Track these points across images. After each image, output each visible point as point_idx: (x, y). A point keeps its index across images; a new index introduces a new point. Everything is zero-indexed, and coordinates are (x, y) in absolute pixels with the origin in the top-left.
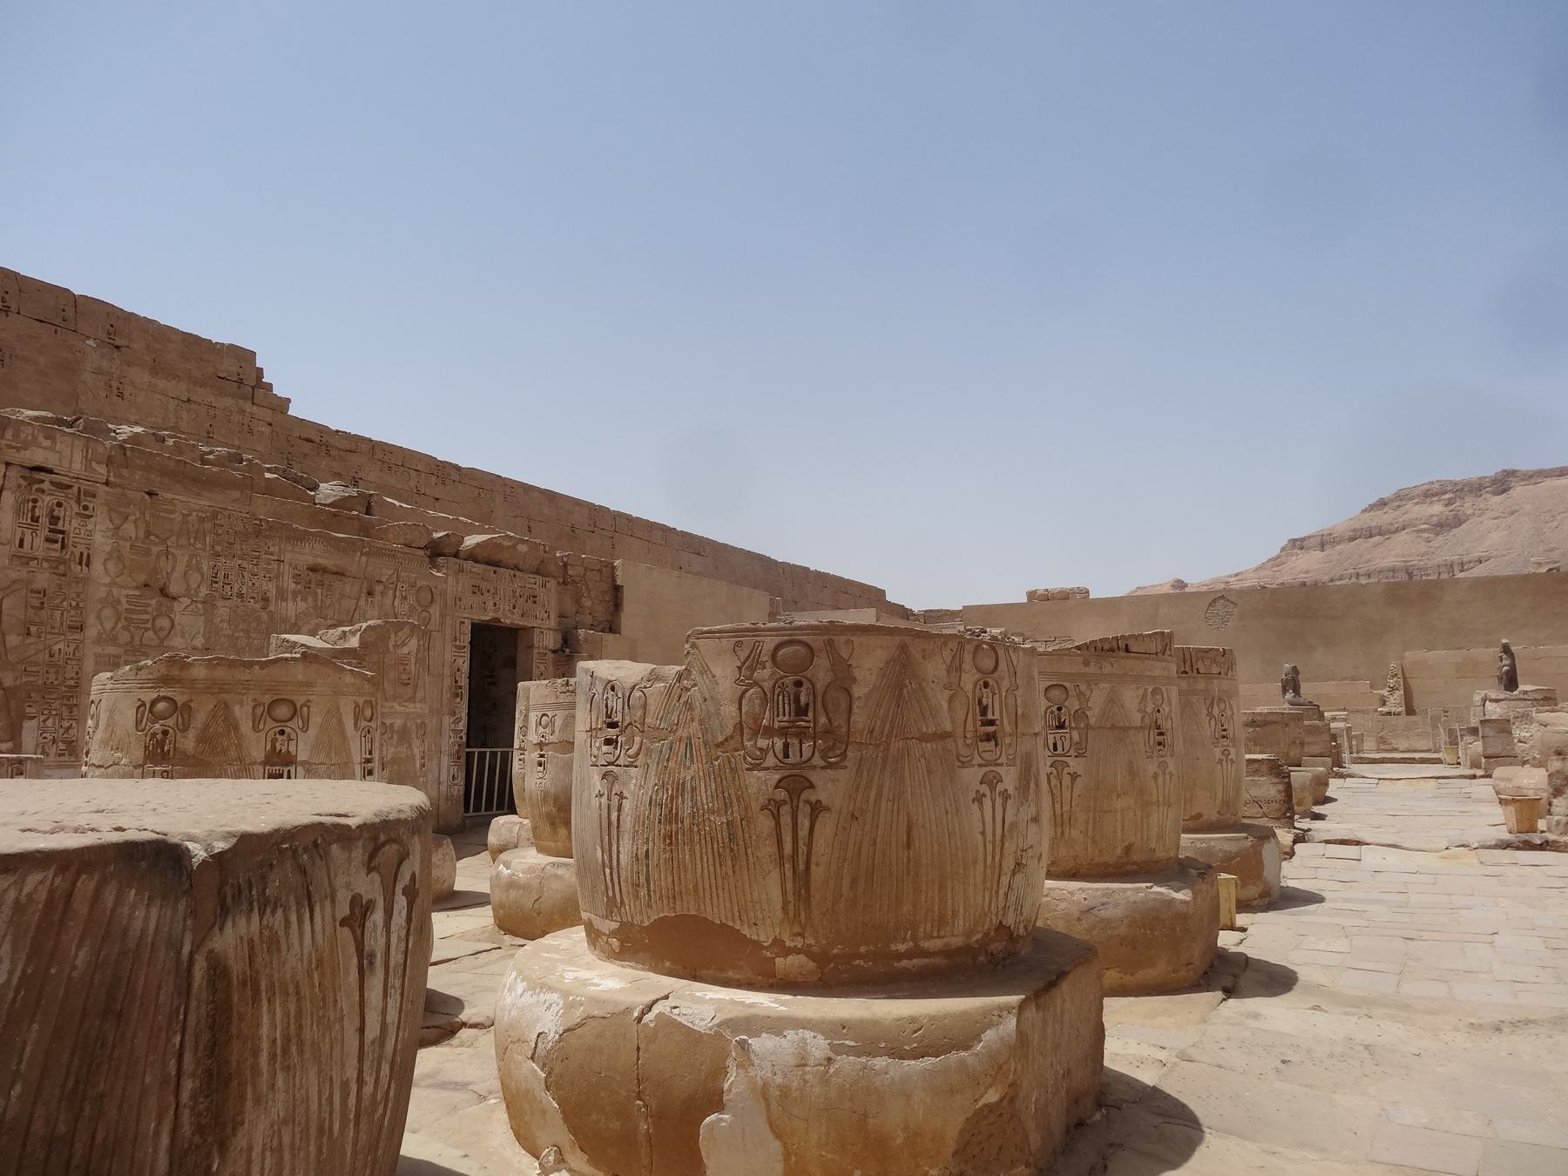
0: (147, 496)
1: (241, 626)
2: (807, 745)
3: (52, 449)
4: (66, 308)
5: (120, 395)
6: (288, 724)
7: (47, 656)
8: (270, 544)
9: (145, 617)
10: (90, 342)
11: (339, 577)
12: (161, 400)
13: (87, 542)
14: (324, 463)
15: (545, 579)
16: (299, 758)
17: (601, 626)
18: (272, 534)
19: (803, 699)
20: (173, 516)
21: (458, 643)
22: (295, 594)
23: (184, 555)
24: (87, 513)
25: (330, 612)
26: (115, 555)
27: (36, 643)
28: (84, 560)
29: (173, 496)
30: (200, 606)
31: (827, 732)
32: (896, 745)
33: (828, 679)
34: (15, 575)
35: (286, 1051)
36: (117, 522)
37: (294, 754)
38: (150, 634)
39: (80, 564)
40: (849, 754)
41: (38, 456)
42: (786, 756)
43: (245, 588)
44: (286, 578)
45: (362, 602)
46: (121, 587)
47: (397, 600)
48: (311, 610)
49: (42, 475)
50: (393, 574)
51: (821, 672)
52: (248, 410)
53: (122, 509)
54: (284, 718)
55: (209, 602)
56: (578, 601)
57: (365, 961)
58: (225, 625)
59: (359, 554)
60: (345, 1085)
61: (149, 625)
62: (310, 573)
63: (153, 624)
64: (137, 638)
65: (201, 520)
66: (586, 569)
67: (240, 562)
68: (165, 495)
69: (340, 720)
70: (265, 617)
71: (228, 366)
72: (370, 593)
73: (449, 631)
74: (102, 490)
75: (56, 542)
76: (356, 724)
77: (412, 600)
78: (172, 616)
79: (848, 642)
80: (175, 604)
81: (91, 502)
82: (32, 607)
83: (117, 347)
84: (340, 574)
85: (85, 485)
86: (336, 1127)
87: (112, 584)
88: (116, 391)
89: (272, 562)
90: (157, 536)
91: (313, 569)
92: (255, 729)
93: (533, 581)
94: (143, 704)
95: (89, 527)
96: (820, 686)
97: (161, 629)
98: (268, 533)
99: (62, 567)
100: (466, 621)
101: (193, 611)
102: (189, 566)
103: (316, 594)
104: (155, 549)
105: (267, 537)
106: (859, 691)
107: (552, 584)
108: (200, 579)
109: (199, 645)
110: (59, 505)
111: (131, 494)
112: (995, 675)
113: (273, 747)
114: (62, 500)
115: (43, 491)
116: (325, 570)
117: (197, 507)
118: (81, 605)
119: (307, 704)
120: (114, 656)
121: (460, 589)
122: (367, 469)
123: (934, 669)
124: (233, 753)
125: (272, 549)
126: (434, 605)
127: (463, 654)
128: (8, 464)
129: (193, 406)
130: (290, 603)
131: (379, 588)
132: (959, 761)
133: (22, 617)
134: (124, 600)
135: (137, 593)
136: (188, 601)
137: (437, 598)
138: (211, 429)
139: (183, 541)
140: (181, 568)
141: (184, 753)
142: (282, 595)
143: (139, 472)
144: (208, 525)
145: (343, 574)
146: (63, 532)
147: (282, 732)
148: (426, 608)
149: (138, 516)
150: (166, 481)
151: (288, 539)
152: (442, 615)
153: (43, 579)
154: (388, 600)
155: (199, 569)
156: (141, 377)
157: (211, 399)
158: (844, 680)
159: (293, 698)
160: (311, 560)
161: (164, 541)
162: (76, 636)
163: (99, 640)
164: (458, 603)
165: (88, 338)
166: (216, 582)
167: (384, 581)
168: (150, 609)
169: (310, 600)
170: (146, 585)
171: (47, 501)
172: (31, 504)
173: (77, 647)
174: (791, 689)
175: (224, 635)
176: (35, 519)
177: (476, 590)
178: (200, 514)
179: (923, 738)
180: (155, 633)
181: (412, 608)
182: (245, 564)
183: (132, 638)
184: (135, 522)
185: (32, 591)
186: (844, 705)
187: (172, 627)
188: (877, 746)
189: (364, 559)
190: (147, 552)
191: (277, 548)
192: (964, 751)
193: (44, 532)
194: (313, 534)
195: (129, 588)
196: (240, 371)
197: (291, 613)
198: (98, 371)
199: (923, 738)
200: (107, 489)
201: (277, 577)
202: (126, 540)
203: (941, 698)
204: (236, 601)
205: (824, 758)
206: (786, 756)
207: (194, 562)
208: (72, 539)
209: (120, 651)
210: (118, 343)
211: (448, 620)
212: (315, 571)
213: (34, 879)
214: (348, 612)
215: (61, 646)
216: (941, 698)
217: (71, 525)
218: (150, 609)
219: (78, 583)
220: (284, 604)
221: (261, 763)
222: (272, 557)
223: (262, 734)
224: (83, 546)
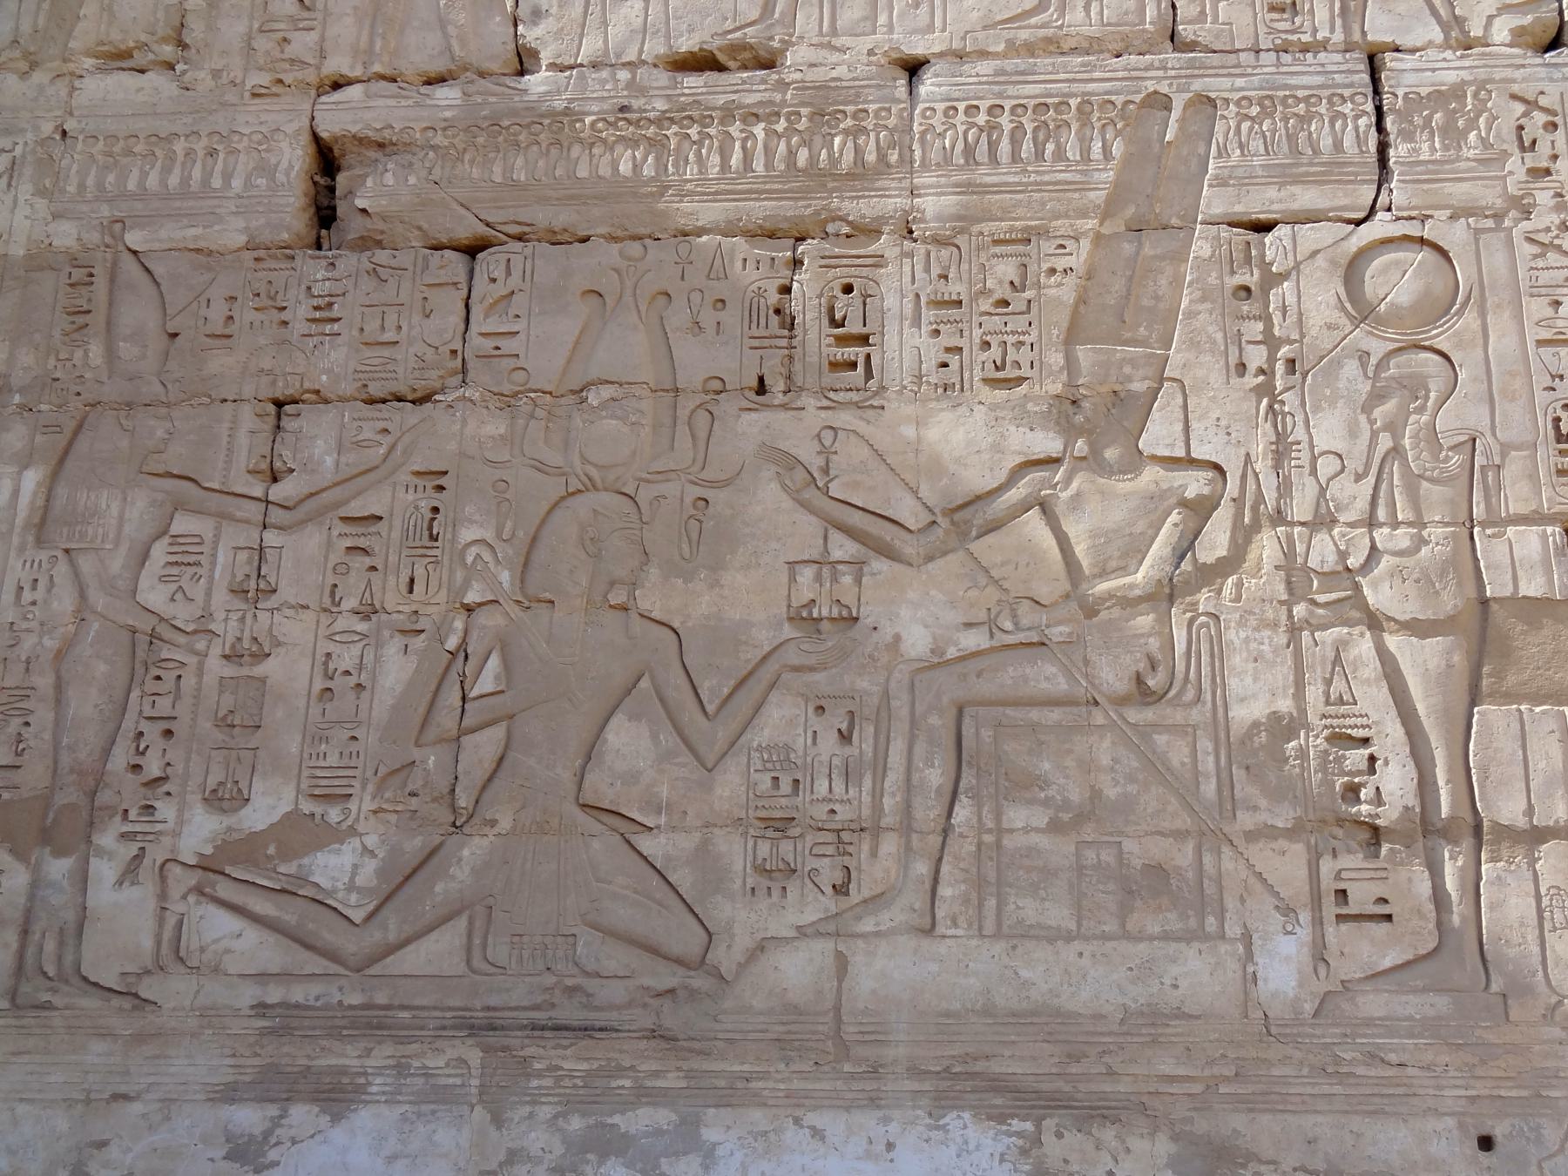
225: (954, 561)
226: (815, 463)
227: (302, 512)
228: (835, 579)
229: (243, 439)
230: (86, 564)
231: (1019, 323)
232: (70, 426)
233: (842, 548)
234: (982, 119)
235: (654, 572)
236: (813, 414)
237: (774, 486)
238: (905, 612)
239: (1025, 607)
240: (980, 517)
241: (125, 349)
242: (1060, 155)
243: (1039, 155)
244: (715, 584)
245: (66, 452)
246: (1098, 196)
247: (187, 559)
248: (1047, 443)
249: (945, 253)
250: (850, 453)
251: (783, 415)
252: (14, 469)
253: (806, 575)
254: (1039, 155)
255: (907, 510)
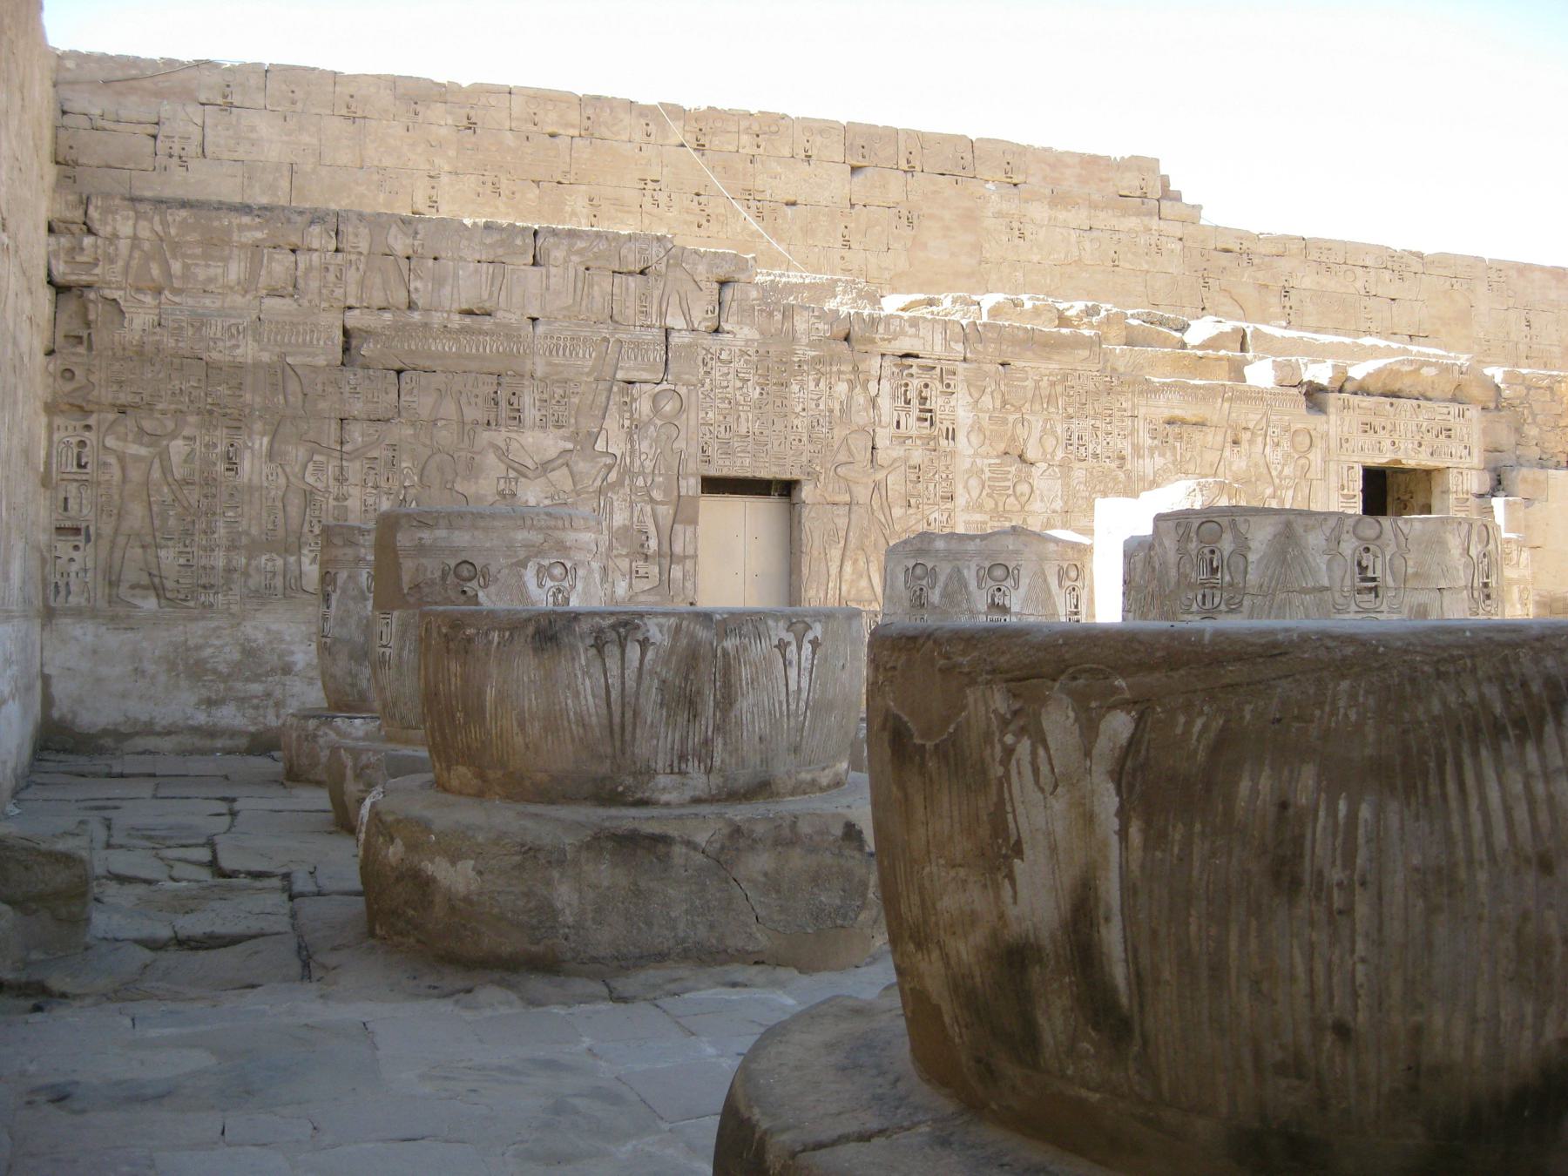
0: (1000, 367)
1: (1098, 488)
2: (1218, 594)
3: (917, 336)
4: (963, 155)
5: (1022, 236)
6: (1004, 583)
7: (925, 525)
8: (1122, 399)
9: (1007, 484)
10: (990, 186)
11: (1200, 428)
12: (1062, 234)
13: (952, 417)
14: (1246, 275)
15: (1461, 407)
16: (1012, 610)
17: (1555, 460)
18: (1124, 389)
19: (1215, 565)
20: (1026, 383)
21: (1345, 492)
22: (1152, 450)
23: (1037, 421)
24: (950, 390)
25: (1191, 467)
26: (977, 427)
27: (916, 514)
28: (951, 435)
29: (1024, 364)
30: (1057, 470)
31: (1231, 585)
32: (1280, 596)
33: (1231, 549)
34: (894, 454)
35: (752, 683)
36: (976, 395)
37: (1008, 606)
38: (1012, 498)
39: (947, 438)
40: (1245, 603)
41: (905, 345)
42: (1204, 604)
43: (1099, 448)
44: (1141, 433)
45: (1227, 453)
46: (983, 457)
47: (1268, 447)
48: (1171, 466)
49: (910, 361)
50: (1261, 418)
51: (1227, 545)
52: (1154, 228)
53: (979, 383)
54: (1001, 578)
55: (1065, 466)
56: (1518, 430)
57: (786, 664)
58: (1082, 487)
59: (1220, 400)
60: (780, 703)
61: (1010, 492)
62: (1167, 426)
63: (1014, 491)
64: (1001, 504)
65: (1053, 384)
66: (1529, 388)
67: (1093, 422)
68: (1016, 363)
69: (1045, 580)
70: (1121, 476)
71: (1129, 183)
72: (1235, 442)
73: (1333, 479)
74: (961, 367)
75: (926, 420)
76: (1060, 585)
77: (1285, 445)
78: (1031, 481)
79: (1248, 521)
80: (1033, 469)
81: (951, 379)
82: (910, 481)
83: (1015, 185)
84: (1201, 424)
85: (946, 365)
86: (778, 715)
87: (976, 454)
88: (1017, 233)
89: (1126, 419)
90: (1012, 405)
91: (1170, 422)
92: (979, 587)
93: (1445, 411)
94: (908, 569)
95: (952, 404)
96: (1226, 554)
97: (1022, 494)
98: (1119, 389)
99: (932, 443)
100: (1355, 465)
101: (1050, 475)
102: (1044, 430)
103: (1175, 448)
104: (1011, 418)
105: (1119, 393)
106: (1252, 557)
107: (1473, 413)
108: (1055, 443)
109: (1058, 508)
110: (926, 386)
111: (987, 367)
112: (1378, 543)
113: (993, 600)
114: (928, 381)
115: (912, 375)
116: (1184, 422)
117: (1047, 372)
118: (950, 476)
119: (1017, 568)
120: (981, 522)
121: (1345, 429)
122: (1300, 275)
123: (1315, 540)
124: (965, 606)
125: (1124, 405)
126: (1314, 449)
127: (1352, 505)
128: (883, 355)
129: (1094, 234)
130: (1147, 460)
131: (1246, 436)
132: (1334, 607)
133: (903, 491)
134: (986, 469)
135: (998, 461)
136: (1045, 466)
137: (1317, 442)
138: (1116, 256)
139: (1037, 407)
140: (1036, 434)
141: (933, 604)
142: (1137, 451)
143: (993, 345)
144: (1059, 389)
145: (1203, 425)
146: (930, 411)
147: (999, 590)
148: (1303, 455)
149: (993, 387)
150: (1017, 349)
151: (1141, 392)
152: (1325, 461)
153: (917, 456)
154: (1258, 448)
155: (1054, 433)
156: (1039, 211)
157: (1114, 222)
158: (1242, 549)
159: (1007, 563)
160: (1167, 414)
161: (1018, 409)
162: (949, 505)
163: (967, 509)
164: (1344, 445)
165: (987, 181)
166: (1071, 445)
167: (1252, 427)
168: (1010, 476)
169: (1168, 454)
170: (1006, 453)
171: (915, 384)
172: (903, 389)
173: (949, 516)
174: (1208, 556)
175: (1083, 498)
176: (908, 402)
177: (1368, 428)
178: (1051, 378)
179: (1304, 591)
180: (1017, 499)
181: (1287, 456)
182: (1098, 424)
183: (996, 504)
184: (992, 393)
185: (910, 467)
186: (1242, 567)
187: (1032, 491)
188: (1265, 596)
189: (1226, 405)
190: (1005, 421)
191: (1130, 403)
192: (1341, 601)
193: (915, 413)
194: (1168, 385)
195: (991, 458)
196: (1143, 184)
197: (1150, 472)
198: (999, 215)
199: (1304, 591)
200: (965, 365)
201: (1131, 434)
202: (984, 412)
203: (1321, 562)
204: (1091, 462)
205: (1227, 605)
206: (1204, 604)
207: (1048, 426)
208: (938, 416)
209: (987, 518)
210: (1015, 181)
211: (1333, 466)
212: (1173, 423)
213: (672, 620)
214: (1211, 465)
215: (936, 515)
216: (1321, 562)
217: (936, 403)
218: (1010, 476)
219: (946, 456)
220: (1141, 461)
221: (985, 613)
222: (1125, 414)
223: (984, 591)
224: (949, 422)
225: (542, 480)
226: (504, 448)
227: (355, 455)
228: (510, 482)
229: (332, 430)
230: (288, 469)
231: (562, 408)
232: (276, 423)
233: (512, 474)
234: (555, 341)
235: (459, 479)
236: (504, 433)
237: (493, 455)
238: (529, 493)
239: (561, 494)
240: (550, 466)
241: (291, 399)
242: (577, 354)
243: (571, 354)
244: (476, 483)
245: (276, 430)
246: (587, 370)
247: (319, 469)
248: (570, 446)
249: (543, 384)
250: (514, 445)
251: (496, 433)
252: (259, 437)
253: (502, 481)
254: (571, 354)
255: (530, 464)
